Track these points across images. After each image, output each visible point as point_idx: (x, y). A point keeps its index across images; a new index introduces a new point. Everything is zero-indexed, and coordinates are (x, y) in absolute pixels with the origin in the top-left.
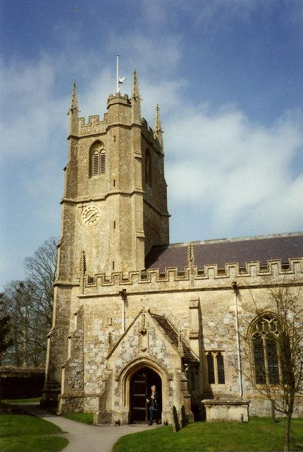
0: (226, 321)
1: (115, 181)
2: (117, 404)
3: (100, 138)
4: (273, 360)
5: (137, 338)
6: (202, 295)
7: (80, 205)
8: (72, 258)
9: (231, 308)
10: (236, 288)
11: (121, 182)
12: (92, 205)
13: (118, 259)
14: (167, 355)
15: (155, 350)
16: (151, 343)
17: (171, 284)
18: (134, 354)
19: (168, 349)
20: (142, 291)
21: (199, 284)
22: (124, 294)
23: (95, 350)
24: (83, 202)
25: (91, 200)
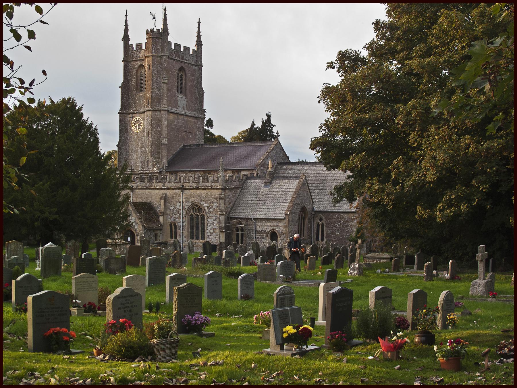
0: (178, 207)
6: (169, 193)
7: (131, 115)
8: (126, 155)
10: (182, 189)
13: (150, 158)
24: (132, 114)
25: (137, 113)
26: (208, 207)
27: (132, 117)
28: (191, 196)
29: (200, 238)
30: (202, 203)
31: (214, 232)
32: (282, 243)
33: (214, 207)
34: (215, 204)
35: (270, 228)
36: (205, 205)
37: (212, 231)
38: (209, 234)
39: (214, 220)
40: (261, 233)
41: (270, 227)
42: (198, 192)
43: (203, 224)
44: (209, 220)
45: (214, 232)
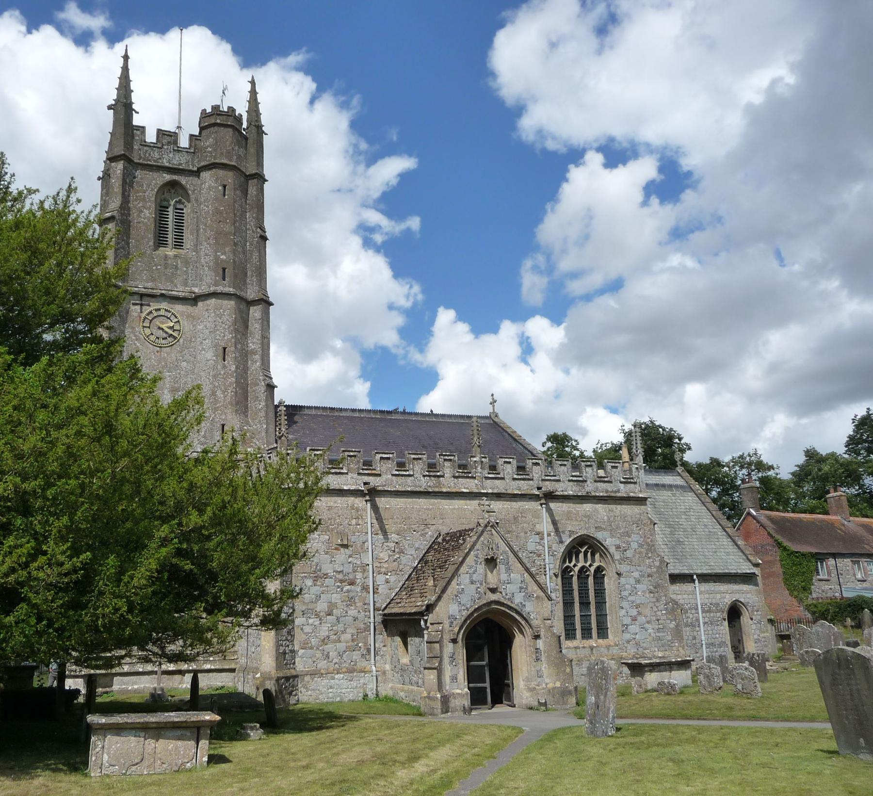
0: (531, 546)
1: (224, 270)
2: (454, 678)
3: (183, 180)
4: (585, 604)
5: (481, 568)
9: (538, 526)
11: (236, 276)
12: (164, 305)
14: (529, 596)
15: (511, 588)
16: (504, 577)
17: (448, 483)
18: (477, 596)
19: (530, 589)
20: (400, 489)
21: (490, 487)
22: (372, 493)
23: (315, 590)
25: (162, 295)
26: (618, 547)
27: (142, 305)
28: (569, 516)
29: (579, 633)
30: (599, 536)
31: (639, 613)
32: (758, 632)
33: (634, 545)
34: (634, 537)
35: (728, 600)
36: (609, 542)
37: (634, 612)
38: (627, 620)
39: (638, 581)
40: (709, 611)
41: (727, 596)
42: (588, 507)
43: (600, 592)
44: (623, 580)
45: (639, 613)
